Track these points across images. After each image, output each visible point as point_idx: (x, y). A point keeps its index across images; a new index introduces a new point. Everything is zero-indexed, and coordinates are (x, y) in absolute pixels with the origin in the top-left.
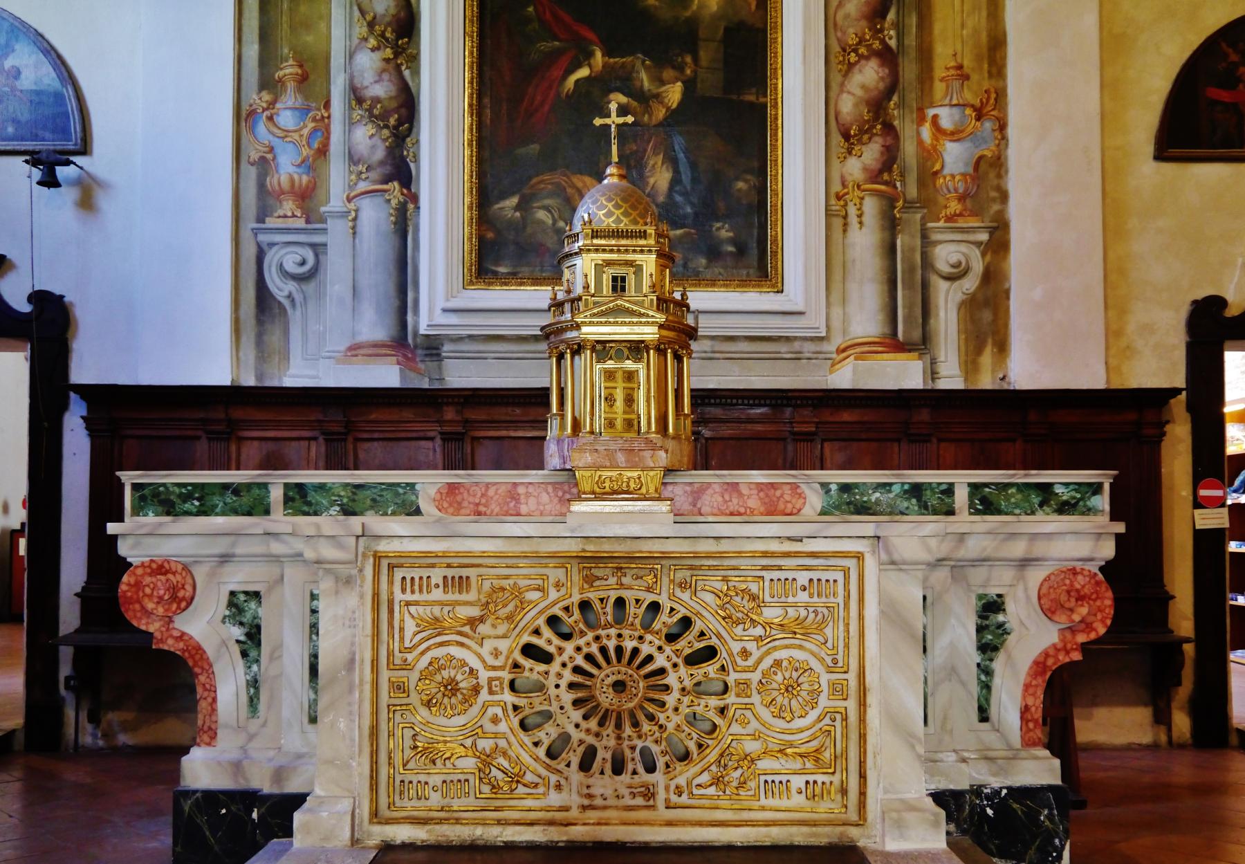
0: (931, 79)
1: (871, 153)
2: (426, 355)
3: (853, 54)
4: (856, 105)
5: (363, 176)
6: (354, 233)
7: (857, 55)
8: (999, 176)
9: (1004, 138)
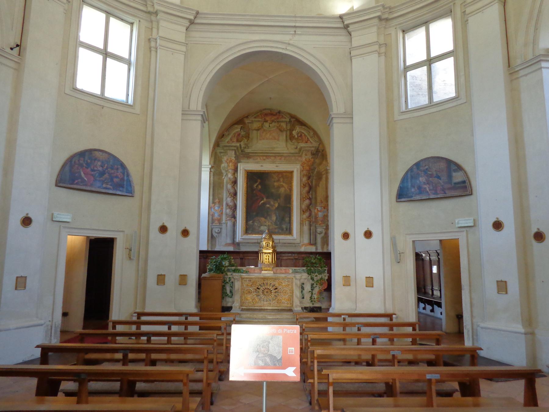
1: (307, 214)
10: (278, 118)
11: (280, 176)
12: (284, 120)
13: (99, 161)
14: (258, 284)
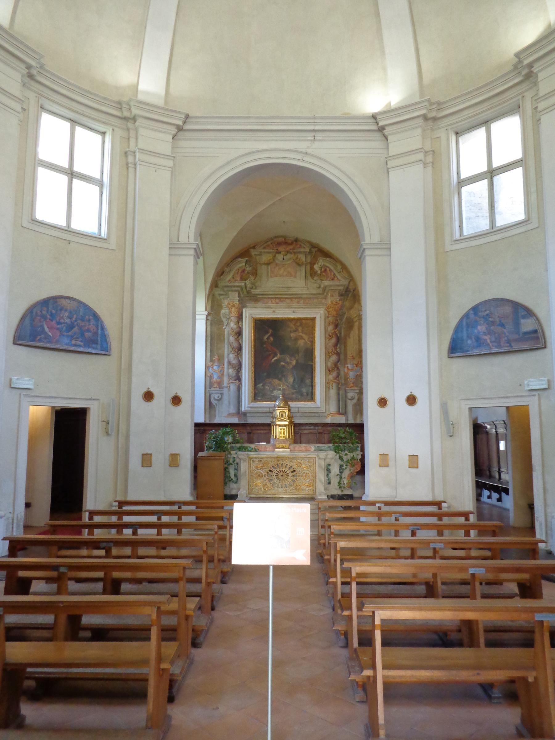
1: (334, 374)
10: (294, 249)
11: (298, 324)
12: (302, 250)
13: (66, 310)
14: (270, 465)
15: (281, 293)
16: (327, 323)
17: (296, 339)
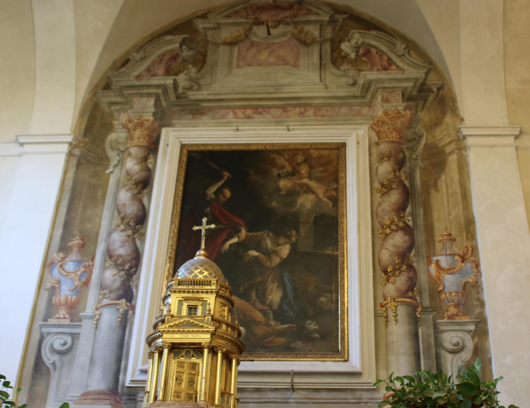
0: (434, 241)
1: (401, 281)
2: (128, 399)
3: (388, 229)
4: (391, 256)
5: (106, 296)
6: (96, 328)
7: (390, 229)
8: (478, 293)
9: (479, 271)
10: (295, 16)
12: (313, 18)
15: (260, 96)
16: (375, 156)
17: (293, 194)
